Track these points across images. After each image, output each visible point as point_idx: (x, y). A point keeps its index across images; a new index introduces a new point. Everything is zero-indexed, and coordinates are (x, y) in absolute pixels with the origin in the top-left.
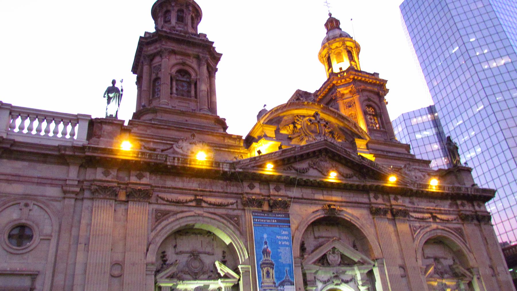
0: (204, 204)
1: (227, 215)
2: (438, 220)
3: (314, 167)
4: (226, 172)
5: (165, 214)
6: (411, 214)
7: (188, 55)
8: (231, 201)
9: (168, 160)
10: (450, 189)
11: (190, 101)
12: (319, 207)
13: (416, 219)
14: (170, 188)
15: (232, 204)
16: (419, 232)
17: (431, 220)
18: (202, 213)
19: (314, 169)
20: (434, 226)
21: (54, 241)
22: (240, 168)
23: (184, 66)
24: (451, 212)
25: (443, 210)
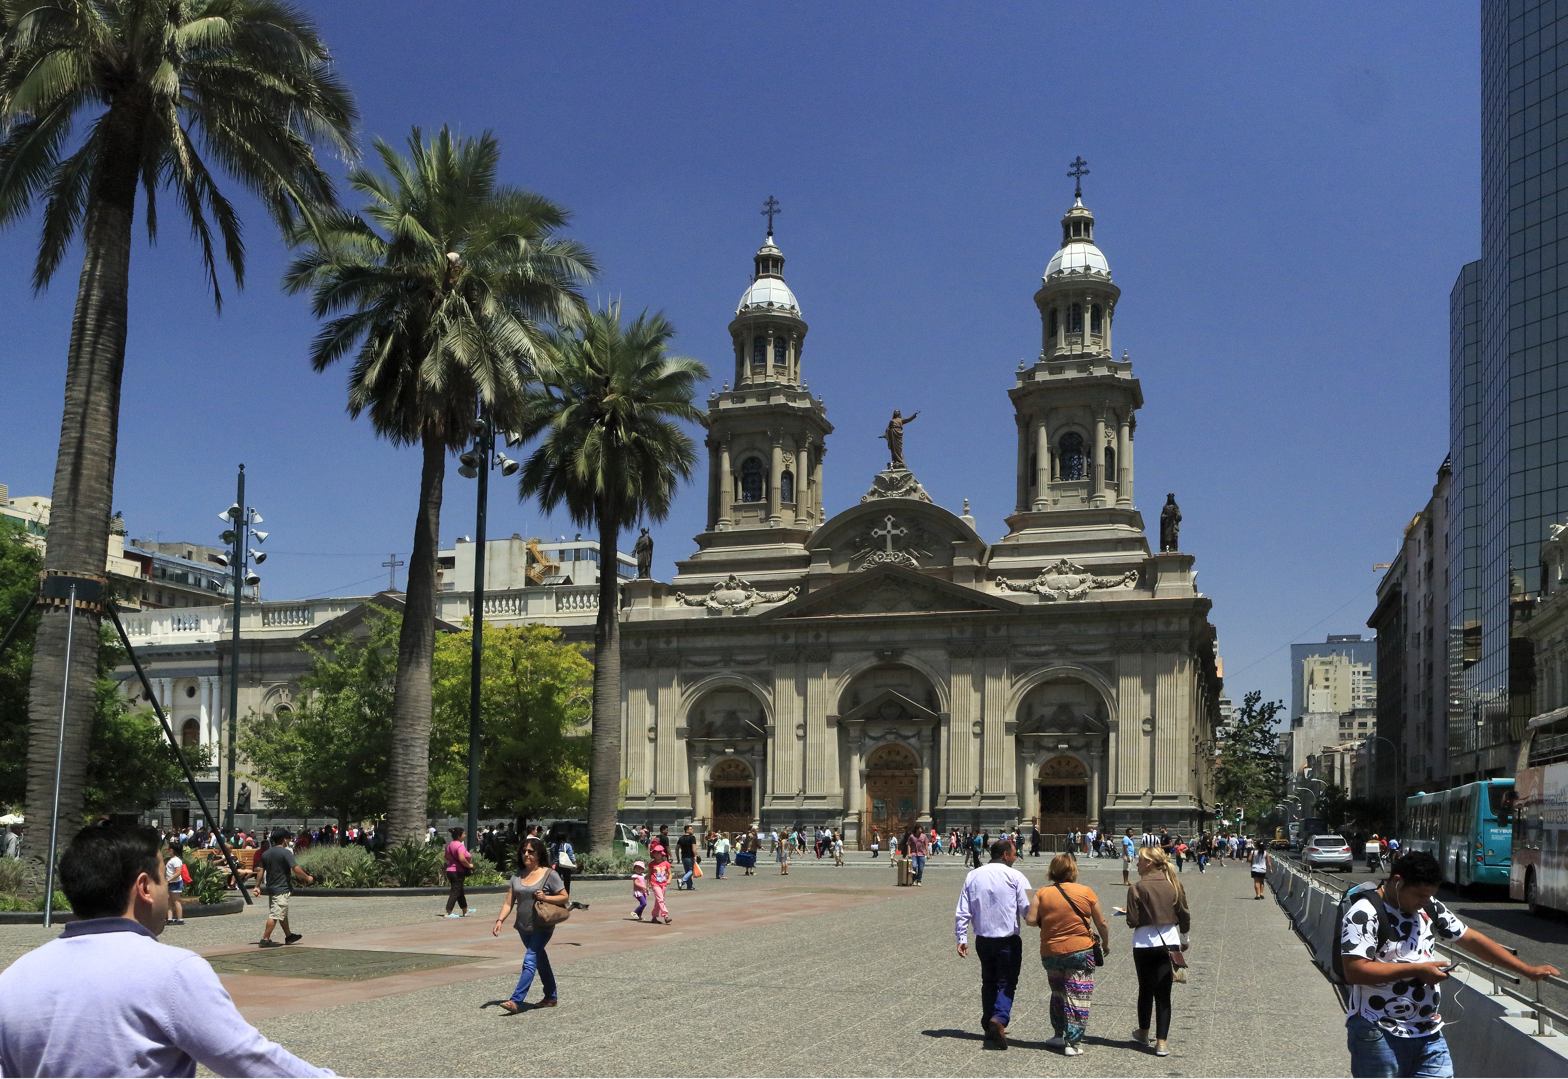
0: (732, 663)
15: (763, 660)
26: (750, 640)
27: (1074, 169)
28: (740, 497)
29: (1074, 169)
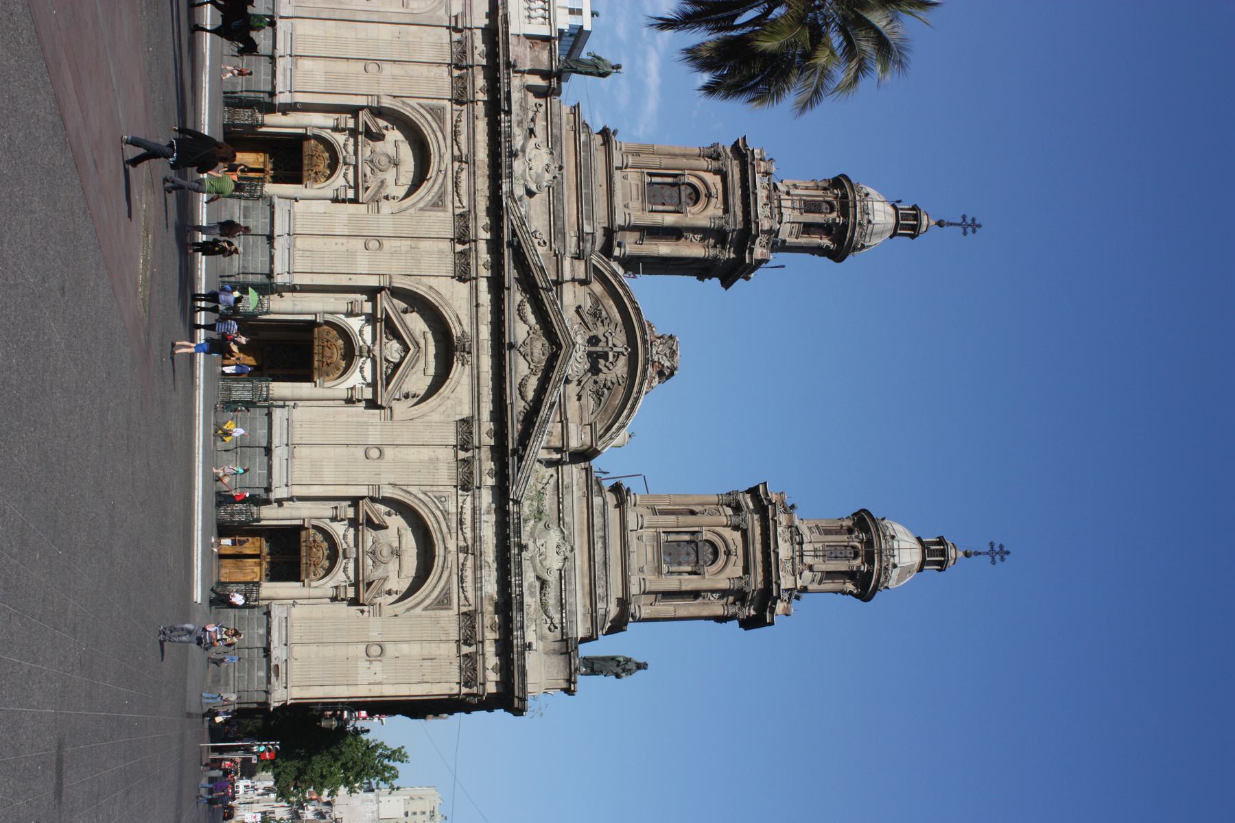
1: (445, 192)
2: (462, 556)
3: (531, 332)
4: (501, 189)
6: (469, 499)
8: (465, 202)
11: (643, 201)
12: (467, 329)
13: (460, 510)
14: (474, 123)
15: (460, 201)
16: (438, 507)
17: (462, 543)
18: (445, 162)
19: (528, 332)
20: (452, 546)
21: (402, 10)
22: (506, 204)
23: (706, 195)
24: (479, 593)
25: (481, 573)
26: (483, 184)
27: (997, 549)
28: (655, 179)
29: (997, 549)
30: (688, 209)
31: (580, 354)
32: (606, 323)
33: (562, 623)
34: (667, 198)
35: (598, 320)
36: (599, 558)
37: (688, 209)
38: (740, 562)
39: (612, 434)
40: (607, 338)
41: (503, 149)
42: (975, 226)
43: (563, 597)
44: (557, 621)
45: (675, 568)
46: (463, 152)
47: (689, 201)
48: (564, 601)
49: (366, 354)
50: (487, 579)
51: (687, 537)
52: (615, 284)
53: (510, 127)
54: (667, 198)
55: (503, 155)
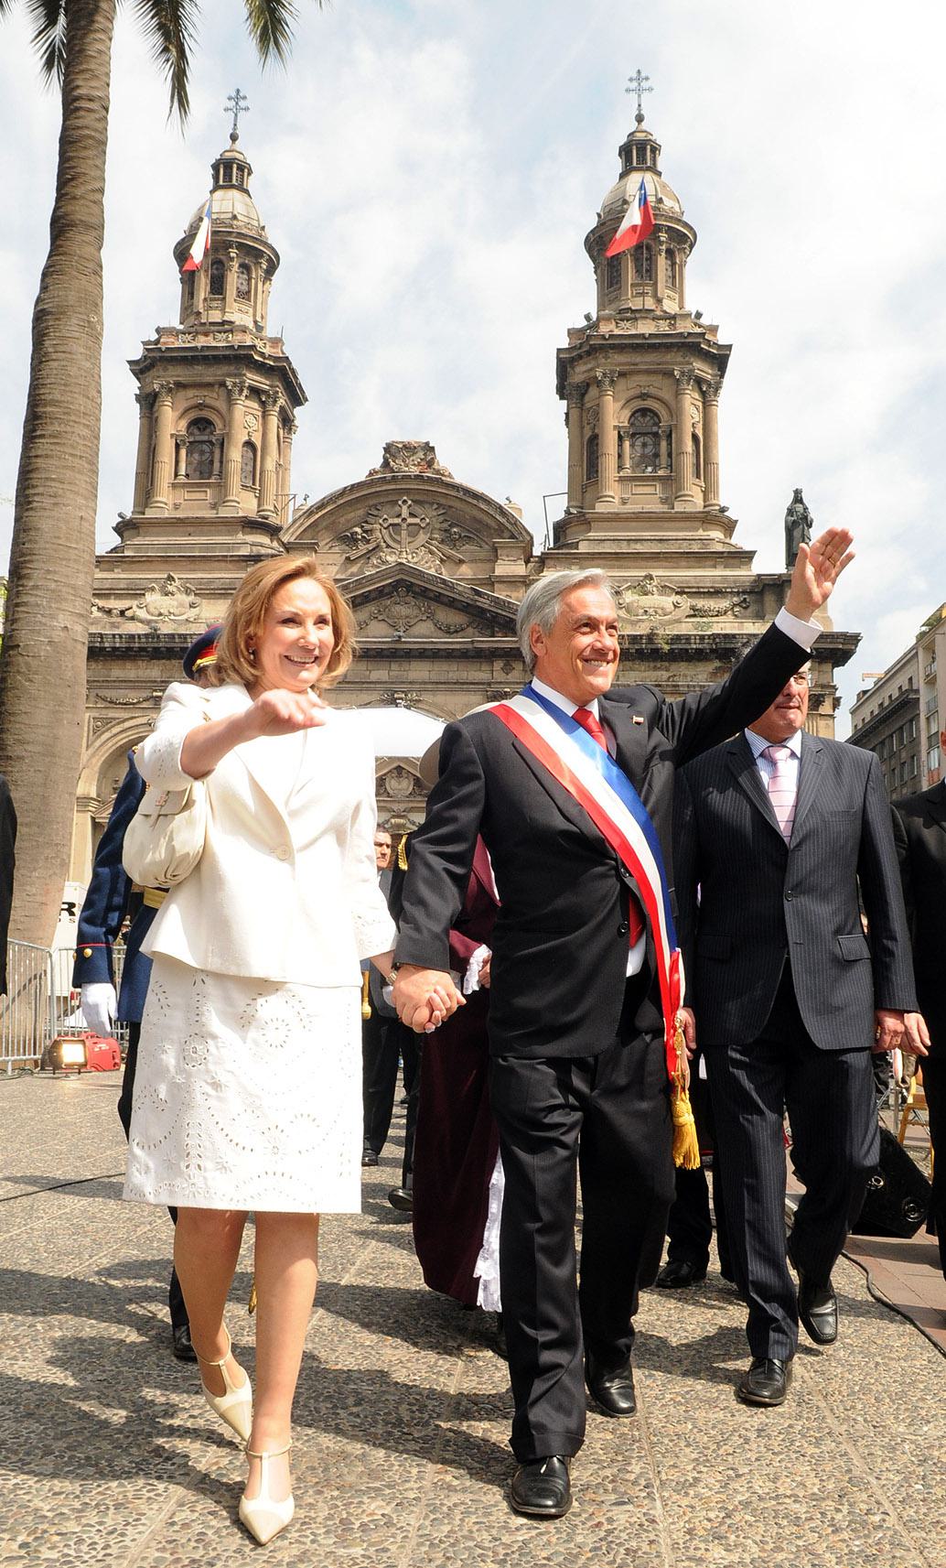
3: (380, 618)
5: (108, 723)
7: (210, 385)
9: (105, 640)
10: (706, 641)
23: (201, 410)
25: (683, 686)
27: (634, 85)
28: (182, 471)
30: (218, 432)
31: (410, 557)
32: (367, 527)
33: (738, 593)
34: (204, 458)
35: (364, 537)
36: (656, 548)
37: (218, 432)
38: (657, 380)
39: (510, 523)
40: (391, 525)
41: (149, 645)
42: (238, 97)
43: (706, 590)
44: (735, 599)
45: (664, 459)
46: (150, 695)
47: (208, 430)
48: (711, 590)
49: (402, 821)
50: (689, 679)
51: (627, 444)
52: (320, 514)
53: (120, 636)
54: (204, 458)
55: (156, 645)
